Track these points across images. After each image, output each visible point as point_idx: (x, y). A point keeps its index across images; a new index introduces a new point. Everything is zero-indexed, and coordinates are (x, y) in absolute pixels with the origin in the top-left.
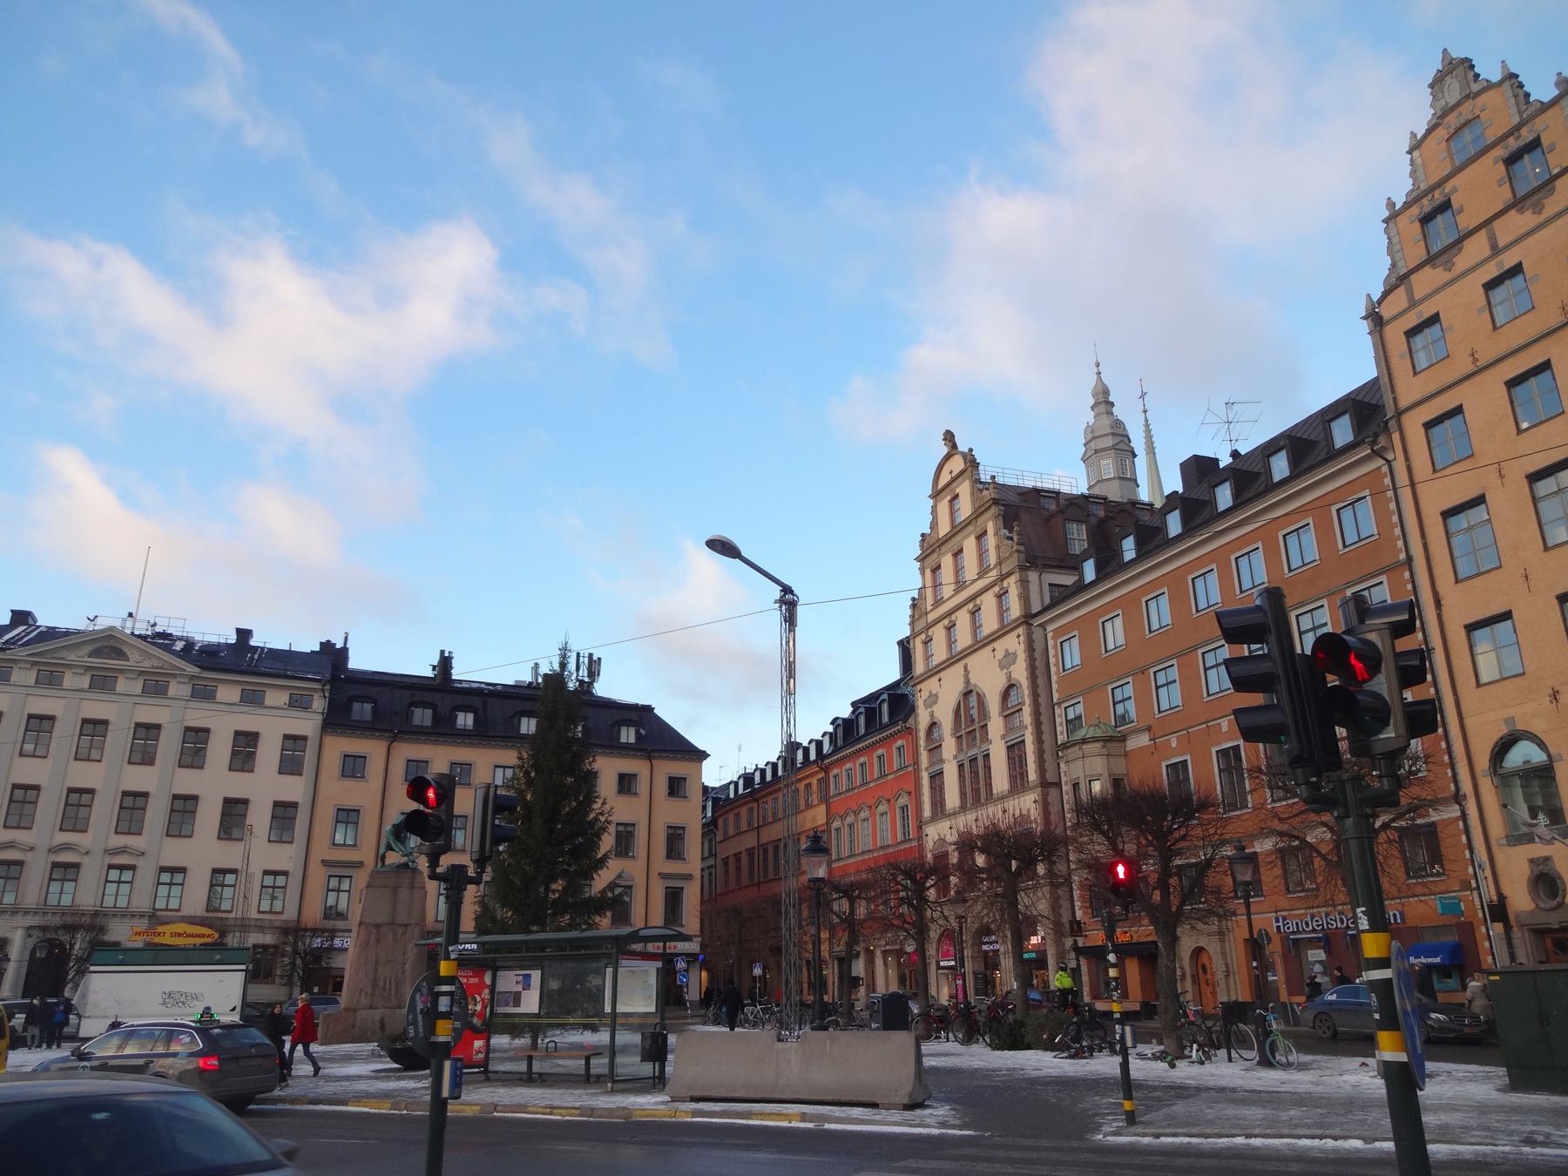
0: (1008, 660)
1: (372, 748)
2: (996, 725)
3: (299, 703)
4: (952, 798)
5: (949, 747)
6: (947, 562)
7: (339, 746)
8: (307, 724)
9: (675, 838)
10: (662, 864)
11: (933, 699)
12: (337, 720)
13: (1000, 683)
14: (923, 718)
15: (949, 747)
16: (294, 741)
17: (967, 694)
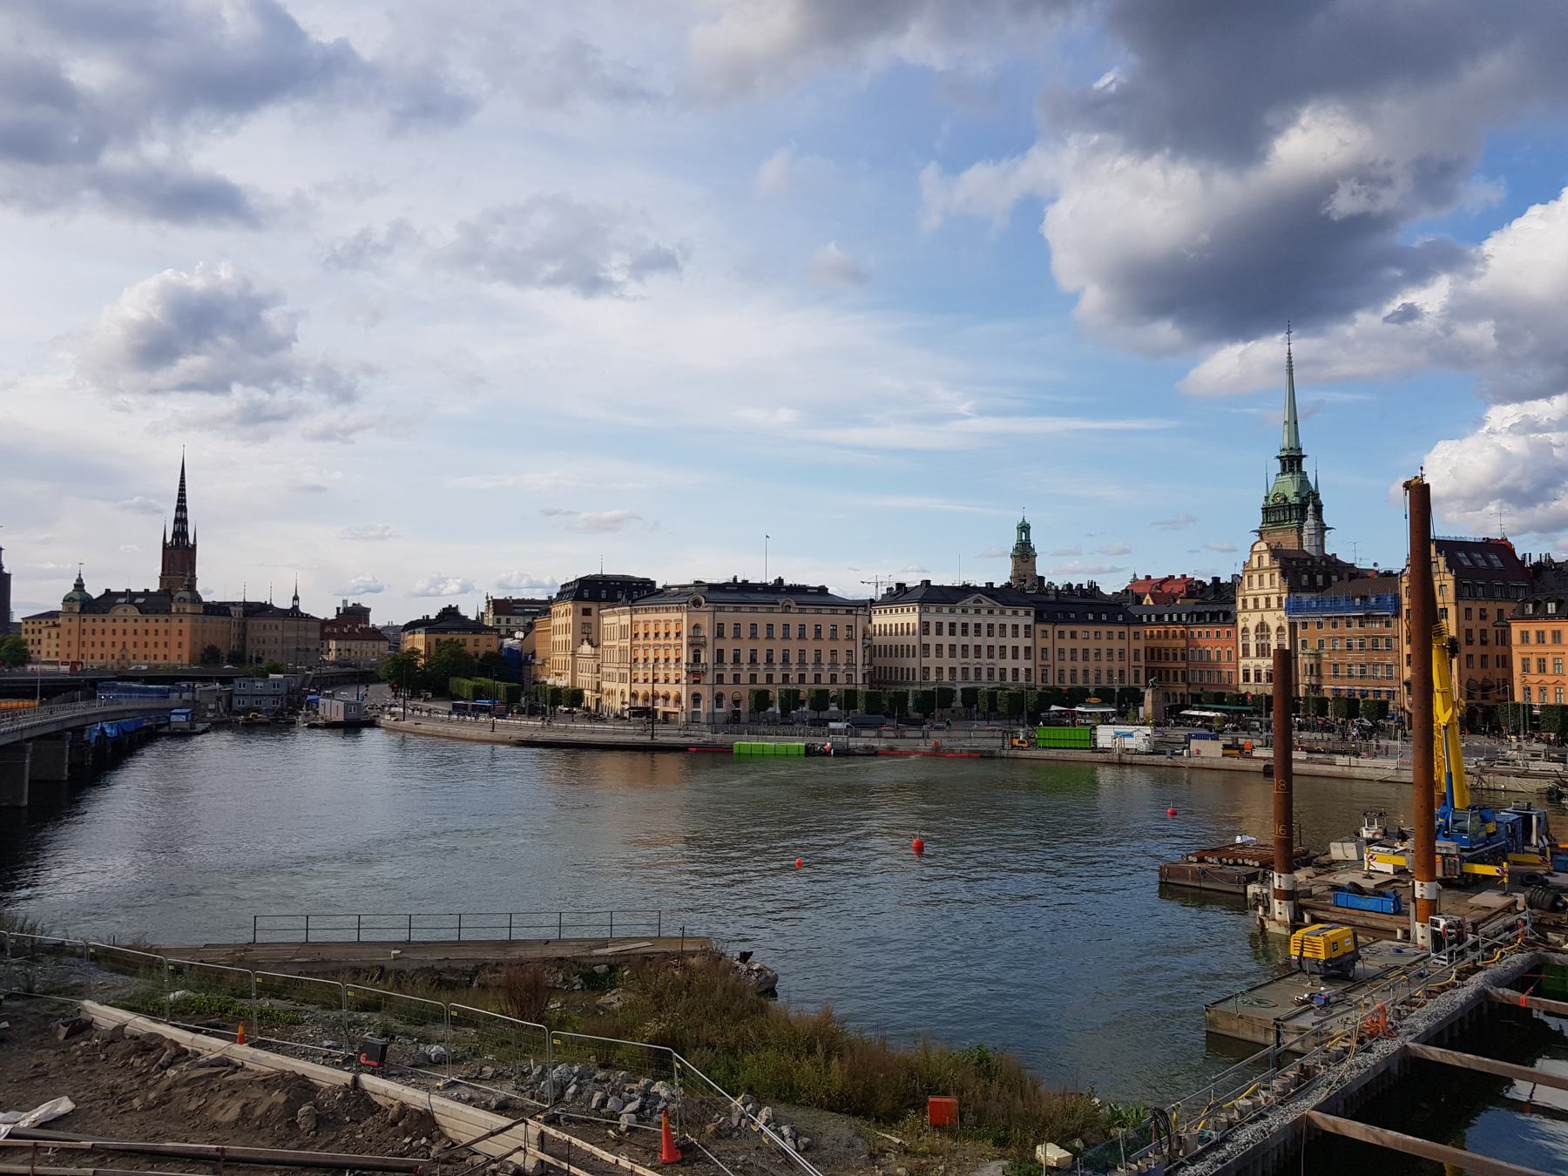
0: (1280, 618)
1: (1048, 627)
2: (1273, 636)
3: (1027, 614)
4: (1253, 652)
5: (1252, 637)
6: (1256, 577)
7: (1040, 627)
8: (1030, 621)
9: (1137, 652)
10: (1133, 663)
11: (1245, 620)
12: (1039, 618)
13: (1277, 624)
14: (1241, 625)
15: (1252, 637)
16: (1027, 627)
17: (1262, 623)
